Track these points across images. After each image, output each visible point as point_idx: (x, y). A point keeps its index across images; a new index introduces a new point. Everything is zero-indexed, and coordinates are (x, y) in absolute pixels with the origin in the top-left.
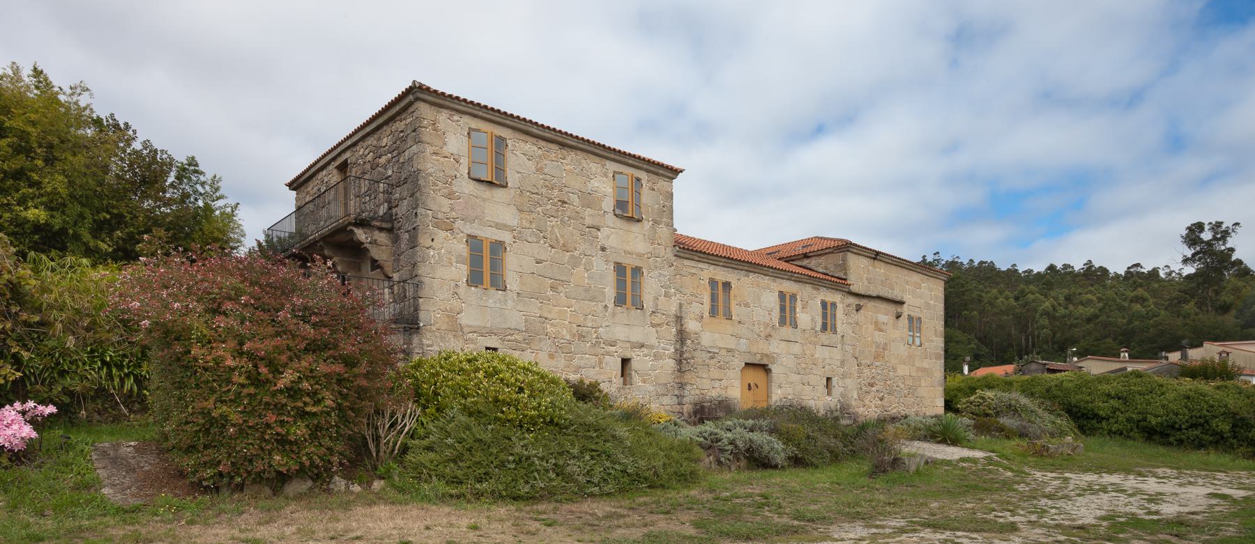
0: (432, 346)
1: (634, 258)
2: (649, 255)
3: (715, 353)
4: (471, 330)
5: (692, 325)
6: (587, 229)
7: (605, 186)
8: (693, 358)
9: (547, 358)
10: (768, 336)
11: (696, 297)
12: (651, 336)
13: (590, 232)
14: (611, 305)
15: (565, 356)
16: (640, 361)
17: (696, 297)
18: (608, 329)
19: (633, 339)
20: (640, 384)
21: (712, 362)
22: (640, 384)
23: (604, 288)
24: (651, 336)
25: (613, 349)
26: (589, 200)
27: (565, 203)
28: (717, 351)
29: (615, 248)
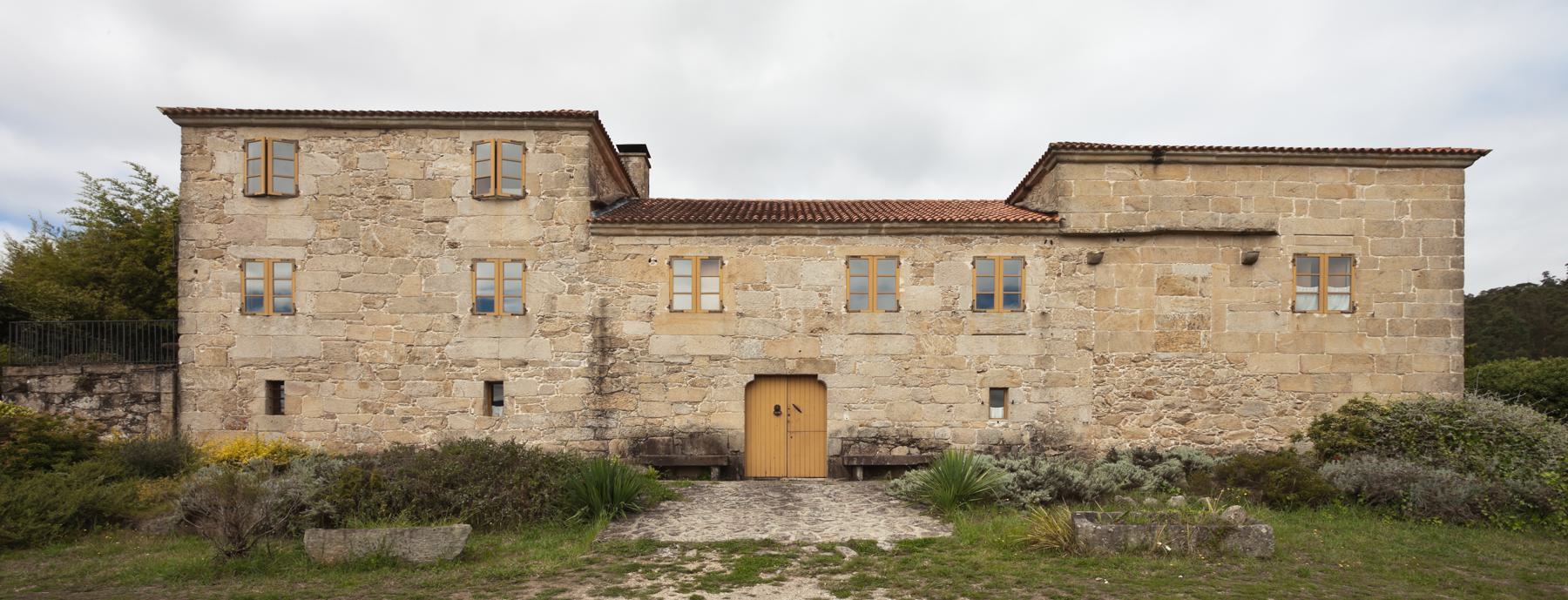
0: (193, 384)
2: (540, 241)
3: (681, 364)
4: (241, 363)
5: (628, 327)
6: (426, 225)
8: (631, 374)
9: (356, 387)
11: (640, 287)
12: (543, 349)
14: (465, 315)
15: (385, 384)
16: (514, 384)
17: (640, 287)
18: (460, 345)
19: (506, 354)
20: (520, 413)
21: (673, 377)
23: (452, 295)
24: (543, 349)
25: (470, 370)
26: (426, 186)
27: (390, 198)
28: (688, 361)
29: (473, 241)
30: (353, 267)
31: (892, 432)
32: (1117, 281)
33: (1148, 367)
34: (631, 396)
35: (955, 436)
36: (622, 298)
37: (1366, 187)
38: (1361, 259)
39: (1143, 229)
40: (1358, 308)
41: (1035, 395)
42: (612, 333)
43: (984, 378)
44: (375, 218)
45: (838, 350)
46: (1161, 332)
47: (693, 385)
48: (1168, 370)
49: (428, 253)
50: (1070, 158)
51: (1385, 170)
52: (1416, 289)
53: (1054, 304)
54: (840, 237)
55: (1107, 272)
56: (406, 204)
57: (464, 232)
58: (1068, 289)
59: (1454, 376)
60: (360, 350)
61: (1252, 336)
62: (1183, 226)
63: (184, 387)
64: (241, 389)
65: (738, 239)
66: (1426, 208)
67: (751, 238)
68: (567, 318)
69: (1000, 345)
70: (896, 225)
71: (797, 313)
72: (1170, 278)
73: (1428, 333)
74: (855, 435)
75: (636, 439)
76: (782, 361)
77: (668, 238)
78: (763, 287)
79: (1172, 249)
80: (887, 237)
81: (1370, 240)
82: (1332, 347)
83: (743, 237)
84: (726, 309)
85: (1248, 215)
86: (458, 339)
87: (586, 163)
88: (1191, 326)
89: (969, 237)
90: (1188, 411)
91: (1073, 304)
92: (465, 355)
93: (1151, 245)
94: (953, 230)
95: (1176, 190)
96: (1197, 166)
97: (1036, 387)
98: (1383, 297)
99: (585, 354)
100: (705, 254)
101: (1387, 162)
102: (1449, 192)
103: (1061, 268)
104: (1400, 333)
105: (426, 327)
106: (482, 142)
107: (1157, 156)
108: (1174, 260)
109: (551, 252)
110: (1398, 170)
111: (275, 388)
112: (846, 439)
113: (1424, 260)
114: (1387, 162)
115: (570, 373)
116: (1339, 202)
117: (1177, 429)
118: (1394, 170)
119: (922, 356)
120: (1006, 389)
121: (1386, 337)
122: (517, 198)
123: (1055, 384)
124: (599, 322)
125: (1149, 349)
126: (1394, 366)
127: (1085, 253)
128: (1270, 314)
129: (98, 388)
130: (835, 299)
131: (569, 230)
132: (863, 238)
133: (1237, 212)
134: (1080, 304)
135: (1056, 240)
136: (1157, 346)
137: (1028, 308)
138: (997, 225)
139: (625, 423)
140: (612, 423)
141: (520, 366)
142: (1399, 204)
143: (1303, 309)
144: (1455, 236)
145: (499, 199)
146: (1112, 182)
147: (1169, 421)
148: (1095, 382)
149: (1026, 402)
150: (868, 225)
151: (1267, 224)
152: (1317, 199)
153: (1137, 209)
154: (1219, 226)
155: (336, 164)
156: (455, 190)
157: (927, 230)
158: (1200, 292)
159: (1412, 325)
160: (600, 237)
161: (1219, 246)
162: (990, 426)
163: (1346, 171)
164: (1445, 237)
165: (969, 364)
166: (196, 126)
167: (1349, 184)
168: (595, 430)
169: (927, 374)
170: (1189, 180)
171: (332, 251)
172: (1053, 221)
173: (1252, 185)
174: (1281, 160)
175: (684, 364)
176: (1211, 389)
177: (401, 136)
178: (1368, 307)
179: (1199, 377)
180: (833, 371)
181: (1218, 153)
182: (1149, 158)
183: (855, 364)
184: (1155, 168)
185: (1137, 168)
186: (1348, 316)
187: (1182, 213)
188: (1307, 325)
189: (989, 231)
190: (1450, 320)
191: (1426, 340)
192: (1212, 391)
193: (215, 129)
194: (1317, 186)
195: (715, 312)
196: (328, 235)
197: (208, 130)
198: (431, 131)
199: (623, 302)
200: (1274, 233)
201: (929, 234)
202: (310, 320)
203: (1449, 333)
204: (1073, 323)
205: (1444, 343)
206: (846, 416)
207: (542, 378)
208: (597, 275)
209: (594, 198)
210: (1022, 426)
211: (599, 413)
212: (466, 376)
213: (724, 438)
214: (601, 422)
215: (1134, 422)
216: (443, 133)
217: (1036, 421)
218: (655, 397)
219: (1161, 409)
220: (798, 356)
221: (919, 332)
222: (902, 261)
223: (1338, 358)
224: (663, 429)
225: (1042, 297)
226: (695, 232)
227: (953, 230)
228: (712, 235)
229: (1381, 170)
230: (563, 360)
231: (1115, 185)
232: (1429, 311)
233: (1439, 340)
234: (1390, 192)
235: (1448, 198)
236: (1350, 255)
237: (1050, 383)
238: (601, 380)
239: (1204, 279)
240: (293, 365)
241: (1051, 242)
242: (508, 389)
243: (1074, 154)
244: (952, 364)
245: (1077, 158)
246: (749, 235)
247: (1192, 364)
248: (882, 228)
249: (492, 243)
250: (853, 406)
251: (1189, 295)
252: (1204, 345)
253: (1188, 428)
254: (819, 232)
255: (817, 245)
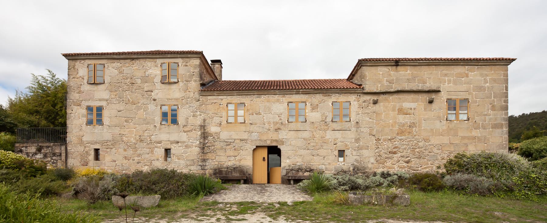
0: (71, 150)
1: (173, 101)
2: (183, 98)
4: (86, 142)
5: (213, 129)
6: (145, 93)
7: (156, 71)
8: (214, 146)
10: (277, 130)
11: (217, 114)
12: (184, 137)
13: (147, 94)
14: (158, 125)
15: (132, 150)
16: (175, 149)
17: (217, 114)
18: (156, 136)
20: (176, 160)
21: (228, 147)
22: (176, 160)
23: (154, 118)
24: (184, 137)
26: (146, 79)
27: (134, 83)
28: (233, 141)
29: (161, 98)
30: (122, 108)
31: (304, 167)
32: (383, 110)
33: (395, 142)
34: (214, 154)
35: (326, 168)
36: (211, 118)
37: (472, 73)
38: (471, 100)
39: (392, 90)
40: (470, 119)
41: (354, 153)
42: (207, 131)
43: (336, 147)
44: (129, 91)
45: (285, 136)
46: (399, 129)
47: (235, 150)
48: (402, 143)
49: (146, 103)
50: (366, 64)
51: (479, 67)
52: (491, 111)
53: (361, 119)
54: (285, 95)
55: (380, 107)
56: (139, 86)
57: (158, 95)
58: (366, 113)
59: (505, 144)
60: (124, 138)
61: (432, 130)
62: (407, 89)
63: (69, 151)
64: (86, 152)
65: (250, 96)
66: (495, 81)
67: (255, 96)
68: (193, 126)
69: (342, 134)
70: (305, 90)
71: (271, 123)
72: (402, 108)
73: (495, 128)
74: (291, 168)
75: (215, 170)
76: (266, 141)
77: (226, 96)
78: (257, 114)
79: (403, 98)
80: (302, 95)
81: (474, 93)
82: (461, 134)
83: (252, 96)
84: (246, 122)
85: (430, 85)
86: (156, 133)
87: (199, 70)
88: (410, 126)
89: (331, 94)
90: (409, 158)
91: (368, 119)
92: (158, 139)
93: (395, 96)
94: (325, 92)
95: (404, 76)
96: (411, 66)
97: (355, 150)
98: (479, 114)
99: (198, 139)
100: (239, 102)
101: (480, 64)
102: (502, 75)
103: (363, 105)
104: (485, 128)
105: (146, 129)
106: (164, 63)
107: (397, 63)
108: (404, 102)
109: (187, 102)
110: (484, 67)
111: (97, 151)
112: (288, 169)
113: (494, 100)
114: (480, 64)
115: (193, 146)
116: (463, 79)
117: (405, 165)
118: (483, 66)
119: (314, 139)
120: (344, 151)
121: (480, 129)
122: (175, 83)
123: (361, 149)
124: (203, 127)
125: (395, 135)
126: (483, 140)
127: (372, 100)
128: (438, 122)
129: (43, 151)
130: (284, 118)
131: (193, 94)
132: (294, 95)
133: (426, 83)
134: (370, 119)
135: (361, 95)
136: (398, 134)
137: (352, 120)
138: (340, 90)
139: (212, 164)
140: (207, 164)
141: (176, 143)
142: (484, 79)
143: (451, 119)
144: (505, 91)
145: (170, 83)
146: (381, 73)
147: (402, 162)
148: (376, 148)
149: (351, 156)
150: (295, 91)
151: (437, 88)
152: (455, 78)
153: (390, 83)
154: (420, 89)
155: (116, 72)
156: (155, 80)
157: (316, 92)
158: (413, 114)
159: (490, 125)
160: (203, 96)
161: (420, 96)
162: (338, 164)
163: (465, 67)
164: (501, 91)
165: (331, 141)
166: (73, 60)
167: (466, 72)
168: (202, 166)
169: (316, 145)
170: (409, 72)
171: (115, 103)
172: (360, 88)
173: (431, 73)
174: (441, 64)
175: (232, 142)
176: (417, 150)
177: (138, 61)
178: (474, 118)
179: (413, 145)
180: (283, 144)
181: (418, 61)
182: (394, 64)
183: (291, 142)
184: (396, 68)
185: (390, 67)
186: (467, 122)
187: (406, 84)
188: (452, 125)
189: (338, 92)
190: (503, 123)
191: (495, 131)
192: (417, 151)
193: (79, 61)
194: (455, 73)
195: (242, 123)
196: (114, 97)
197: (76, 61)
198: (147, 59)
199: (211, 120)
200: (439, 91)
201: (317, 93)
202: (108, 127)
203: (503, 128)
204: (368, 126)
205: (501, 131)
206: (288, 161)
207: (184, 148)
208: (202, 110)
209: (201, 82)
210: (350, 164)
211: (203, 160)
212: (159, 147)
213: (245, 169)
214: (203, 164)
215: (390, 163)
216: (151, 60)
217: (355, 163)
218: (222, 154)
219: (399, 158)
220: (271, 139)
221: (313, 130)
222: (307, 103)
223: (463, 138)
224: (225, 166)
225: (357, 116)
226: (235, 94)
227: (325, 92)
228: (241, 95)
229: (478, 67)
230: (191, 141)
231: (382, 74)
232: (496, 119)
233: (499, 131)
234: (482, 75)
235: (502, 77)
236: (467, 99)
237: (360, 148)
238: (203, 148)
239: (414, 109)
240: (103, 143)
241: (360, 96)
242: (172, 151)
243: (367, 63)
244: (325, 141)
245: (368, 64)
246: (254, 95)
247: (410, 141)
248: (300, 92)
249: (167, 99)
250: (290, 157)
251: (409, 115)
252: (415, 134)
253: (409, 165)
254: (278, 93)
255: (277, 98)
